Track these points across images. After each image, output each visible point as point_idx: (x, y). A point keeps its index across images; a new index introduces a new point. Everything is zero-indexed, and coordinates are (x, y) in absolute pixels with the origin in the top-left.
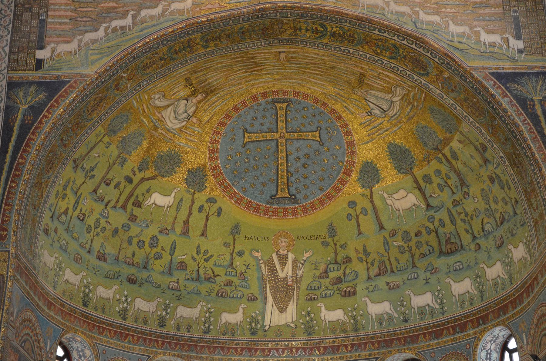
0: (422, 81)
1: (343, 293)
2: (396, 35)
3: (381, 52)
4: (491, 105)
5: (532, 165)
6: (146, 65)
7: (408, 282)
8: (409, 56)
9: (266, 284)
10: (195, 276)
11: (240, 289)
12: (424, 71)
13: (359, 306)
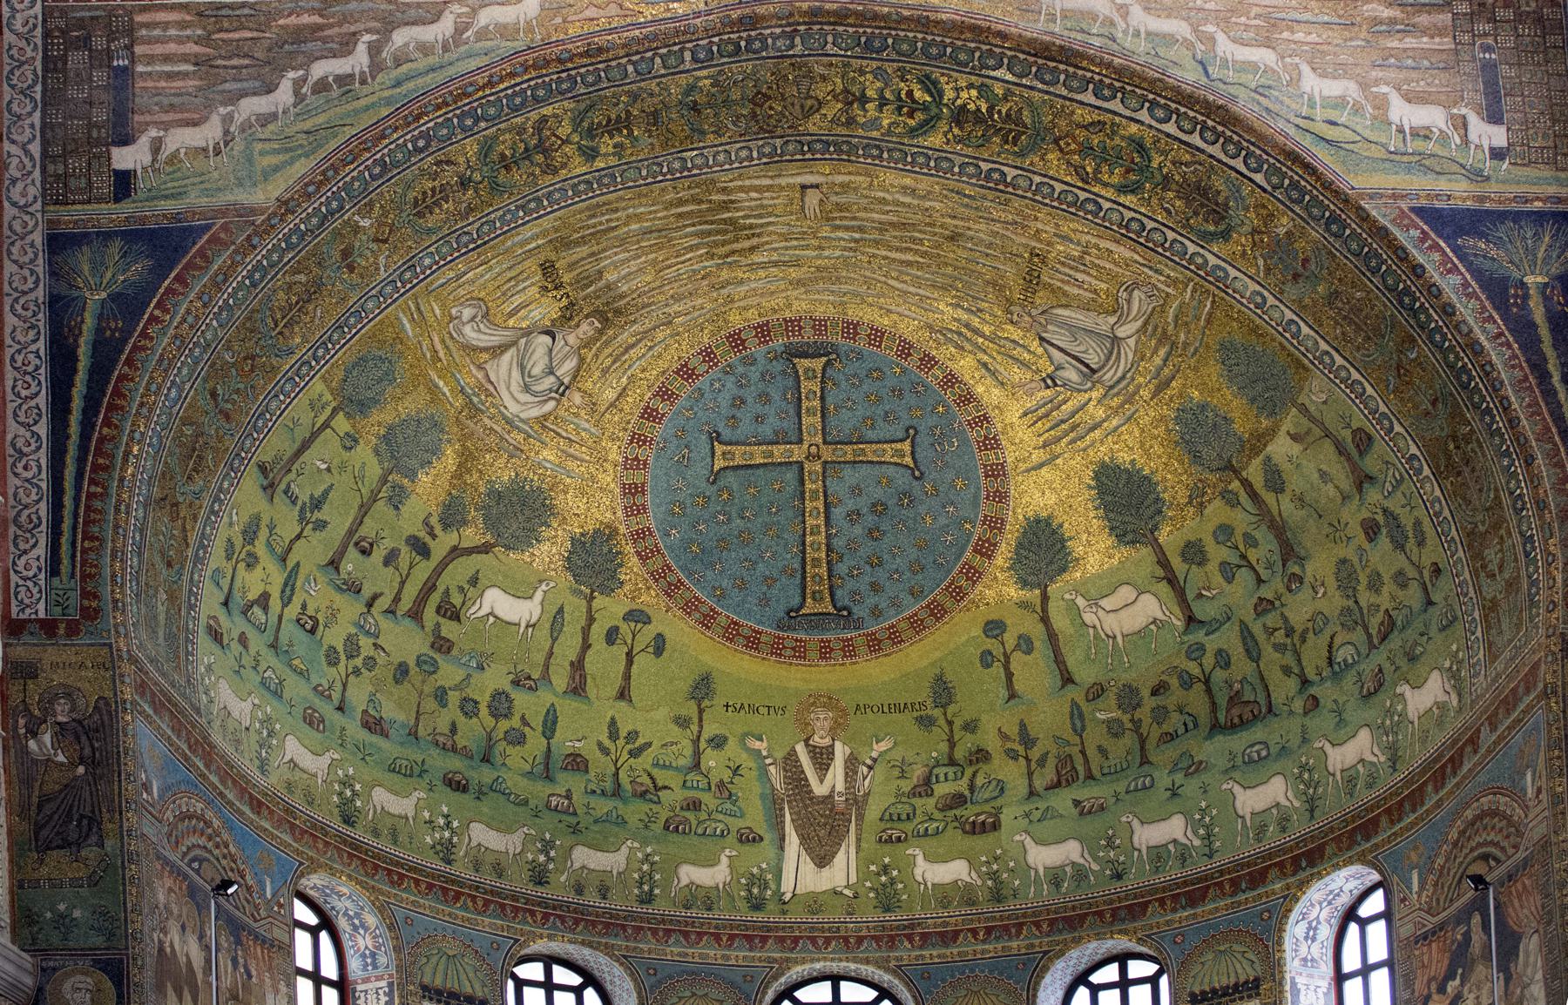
0: (1210, 257)
1: (968, 827)
2: (1147, 105)
3: (1097, 171)
4: (1407, 300)
6: (424, 201)
7: (1127, 797)
8: (1177, 177)
9: (782, 809)
10: (609, 785)
11: (721, 817)
12: (1216, 224)
13: (1005, 852)
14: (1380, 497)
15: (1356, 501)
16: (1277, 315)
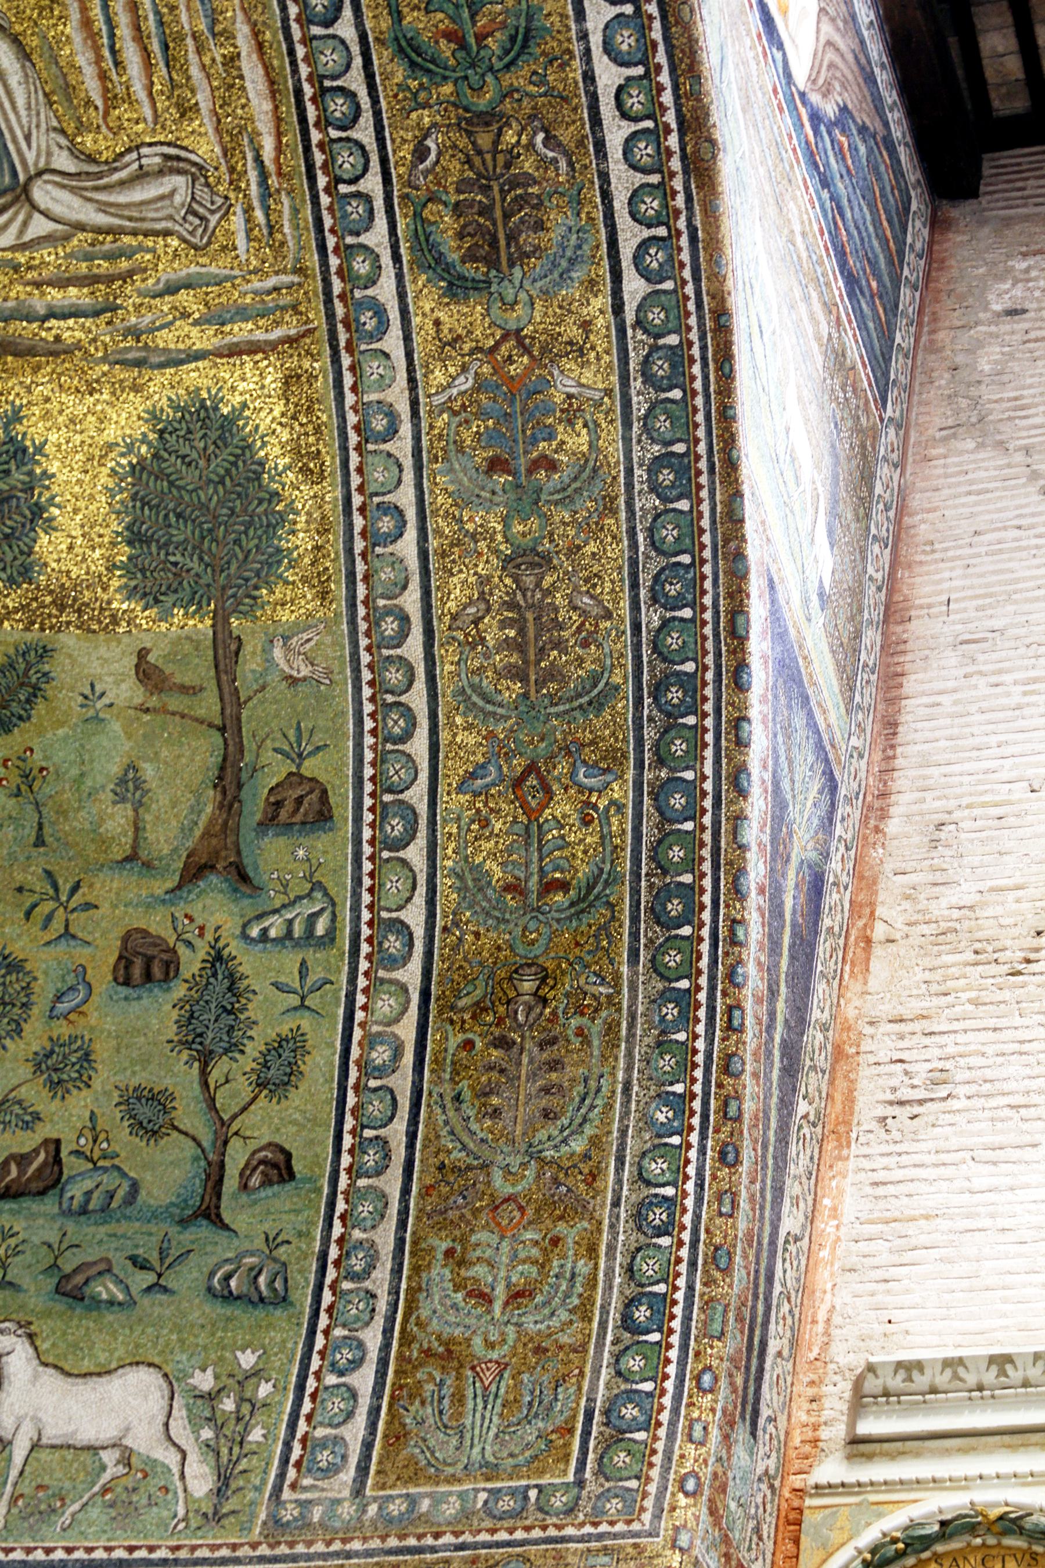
4: (675, 695)
5: (681, 1104)
8: (510, 137)
14: (231, 926)
15: (160, 886)
16: (379, 475)
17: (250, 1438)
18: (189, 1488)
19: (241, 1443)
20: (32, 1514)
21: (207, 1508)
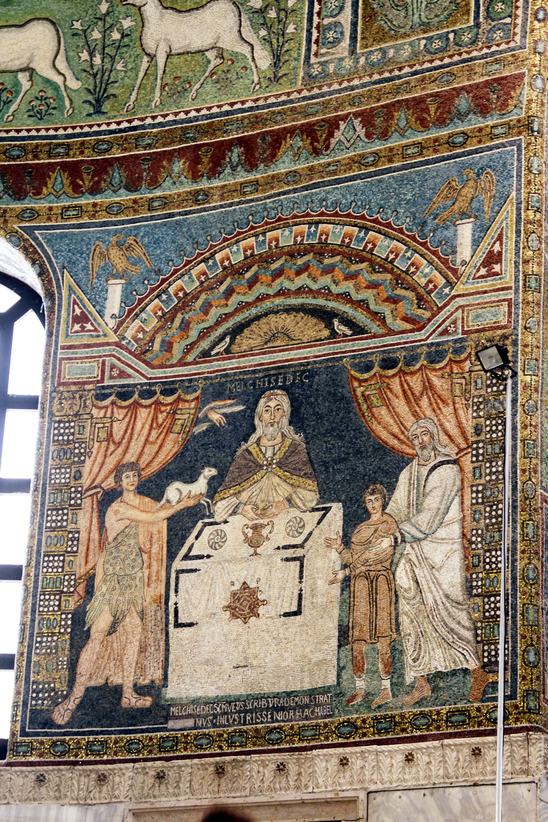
17: (288, 31)
18: (258, 65)
19: (283, 35)
20: (174, 94)
21: (270, 75)
